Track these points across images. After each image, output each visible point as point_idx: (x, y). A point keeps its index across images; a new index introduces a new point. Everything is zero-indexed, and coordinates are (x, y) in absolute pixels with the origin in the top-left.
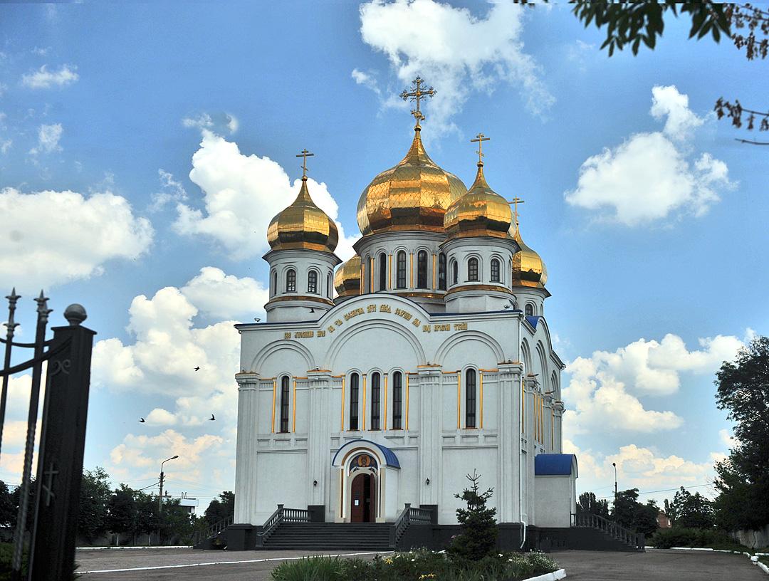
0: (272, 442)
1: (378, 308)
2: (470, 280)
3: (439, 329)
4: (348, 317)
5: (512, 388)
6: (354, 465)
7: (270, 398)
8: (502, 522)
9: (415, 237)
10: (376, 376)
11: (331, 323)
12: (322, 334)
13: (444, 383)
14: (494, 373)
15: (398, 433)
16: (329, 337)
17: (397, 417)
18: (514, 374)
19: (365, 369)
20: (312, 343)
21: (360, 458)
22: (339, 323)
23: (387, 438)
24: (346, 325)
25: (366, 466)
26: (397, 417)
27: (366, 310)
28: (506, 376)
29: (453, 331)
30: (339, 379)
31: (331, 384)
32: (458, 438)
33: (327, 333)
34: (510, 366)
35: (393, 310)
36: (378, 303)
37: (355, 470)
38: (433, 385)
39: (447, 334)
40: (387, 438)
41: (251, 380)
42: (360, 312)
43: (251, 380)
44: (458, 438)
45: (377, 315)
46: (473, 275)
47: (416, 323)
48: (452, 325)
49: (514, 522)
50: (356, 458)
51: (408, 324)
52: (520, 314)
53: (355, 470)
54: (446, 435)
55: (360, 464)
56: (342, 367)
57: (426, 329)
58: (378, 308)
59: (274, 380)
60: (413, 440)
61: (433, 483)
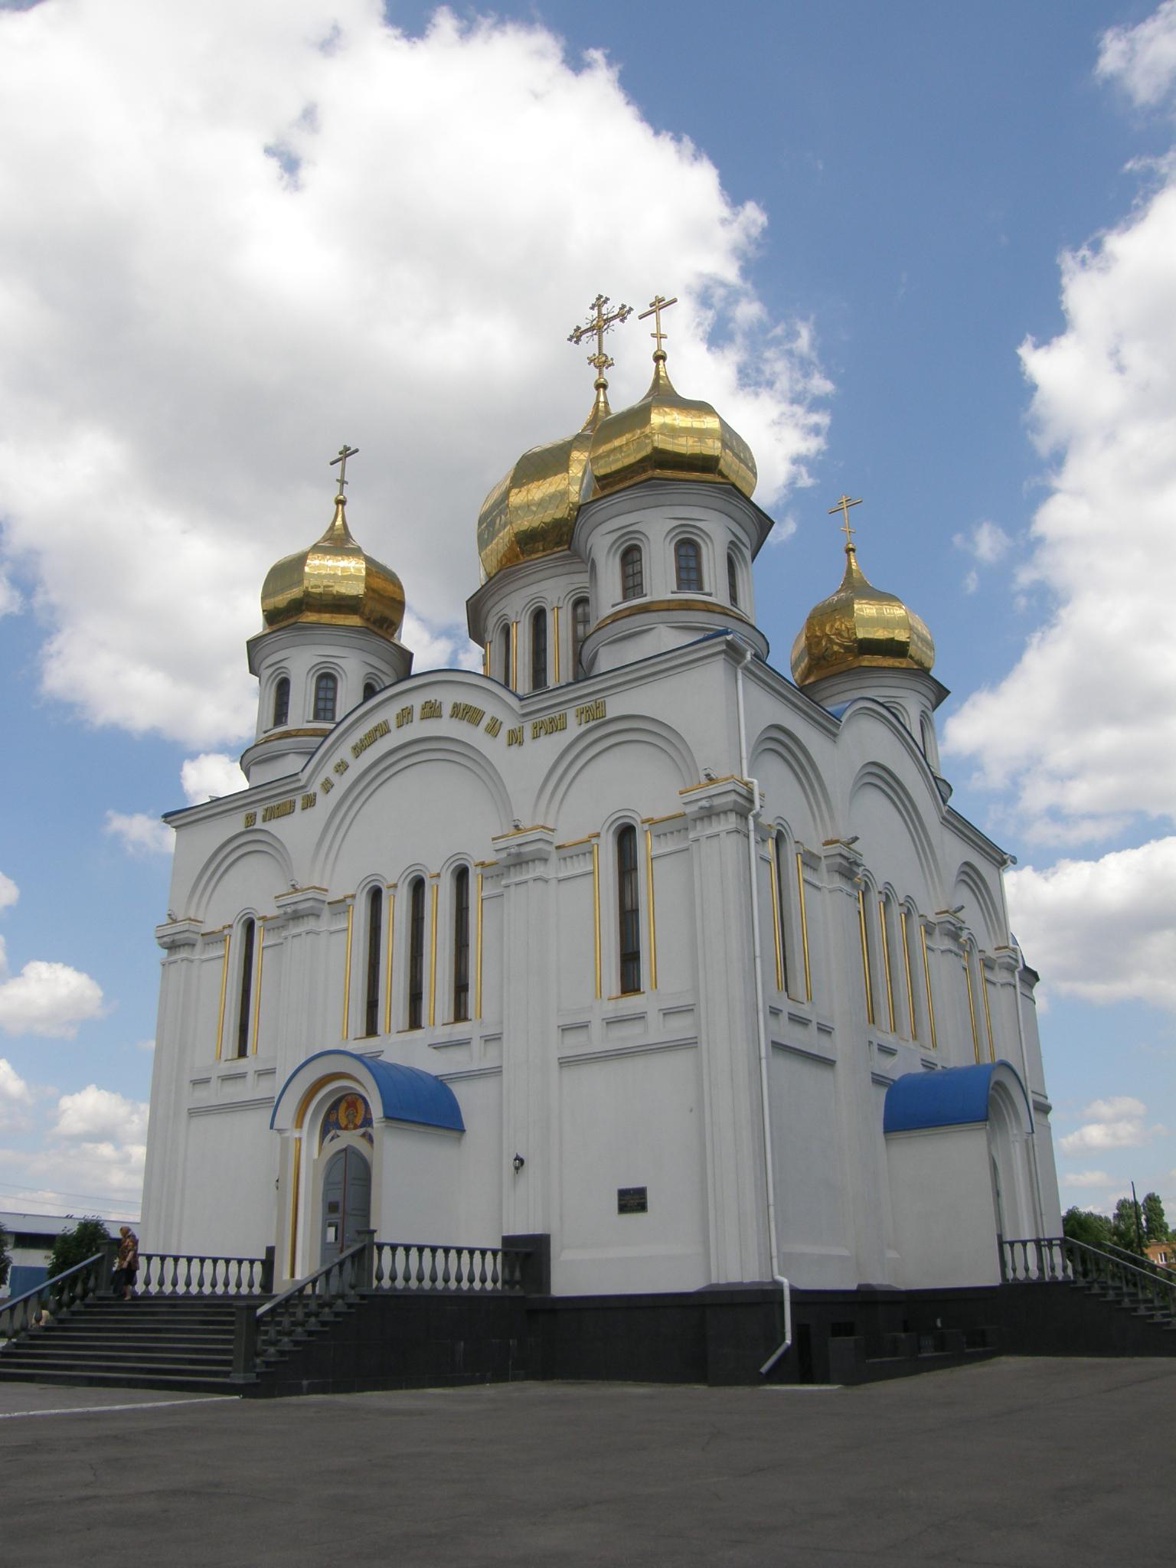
0: (215, 1083)
1: (417, 713)
2: (625, 598)
3: (543, 731)
4: (358, 750)
5: (721, 850)
6: (329, 1126)
7: (214, 975)
8: (714, 1281)
9: (560, 570)
10: (418, 886)
11: (328, 771)
12: (310, 802)
13: (561, 875)
14: (676, 825)
15: (462, 1030)
16: (325, 803)
17: (461, 987)
18: (725, 812)
19: (394, 875)
20: (295, 830)
21: (343, 1105)
22: (342, 767)
23: (437, 1047)
24: (358, 766)
25: (356, 1127)
26: (461, 987)
27: (393, 724)
28: (706, 820)
29: (574, 729)
30: (341, 906)
31: (325, 924)
32: (597, 1027)
33: (321, 798)
34: (714, 789)
35: (447, 710)
36: (417, 701)
37: (333, 1138)
38: (531, 883)
39: (559, 741)
40: (437, 1047)
41: (182, 936)
42: (382, 730)
43: (182, 936)
44: (597, 1027)
45: (419, 728)
46: (632, 583)
47: (493, 729)
48: (572, 719)
49: (747, 1280)
50: (335, 1106)
51: (474, 735)
52: (729, 643)
53: (333, 1138)
54: (568, 1021)
55: (343, 1122)
56: (345, 880)
57: (515, 739)
58: (417, 713)
59: (226, 932)
60: (493, 1048)
61: (509, 1163)
